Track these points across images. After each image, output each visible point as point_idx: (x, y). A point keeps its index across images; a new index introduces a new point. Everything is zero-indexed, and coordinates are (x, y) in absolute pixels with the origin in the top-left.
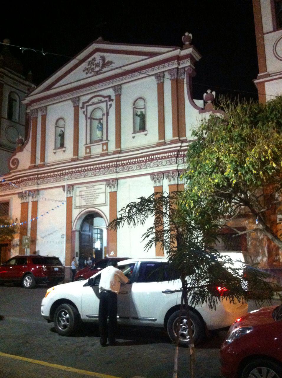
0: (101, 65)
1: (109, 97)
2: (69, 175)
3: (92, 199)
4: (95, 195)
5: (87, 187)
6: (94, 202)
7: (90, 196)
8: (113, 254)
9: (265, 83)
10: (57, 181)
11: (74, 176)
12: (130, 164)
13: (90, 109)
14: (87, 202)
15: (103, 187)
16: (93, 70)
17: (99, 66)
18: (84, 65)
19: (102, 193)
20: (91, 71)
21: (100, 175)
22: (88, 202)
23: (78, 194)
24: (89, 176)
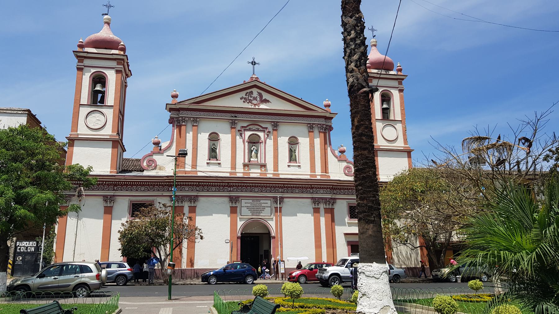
0: (258, 99)
1: (267, 128)
2: (234, 187)
3: (258, 211)
4: (261, 208)
5: (253, 200)
6: (260, 214)
7: (256, 209)
9: (378, 151)
13: (248, 134)
16: (250, 101)
17: (257, 100)
18: (243, 94)
19: (268, 207)
20: (248, 101)
21: (266, 192)
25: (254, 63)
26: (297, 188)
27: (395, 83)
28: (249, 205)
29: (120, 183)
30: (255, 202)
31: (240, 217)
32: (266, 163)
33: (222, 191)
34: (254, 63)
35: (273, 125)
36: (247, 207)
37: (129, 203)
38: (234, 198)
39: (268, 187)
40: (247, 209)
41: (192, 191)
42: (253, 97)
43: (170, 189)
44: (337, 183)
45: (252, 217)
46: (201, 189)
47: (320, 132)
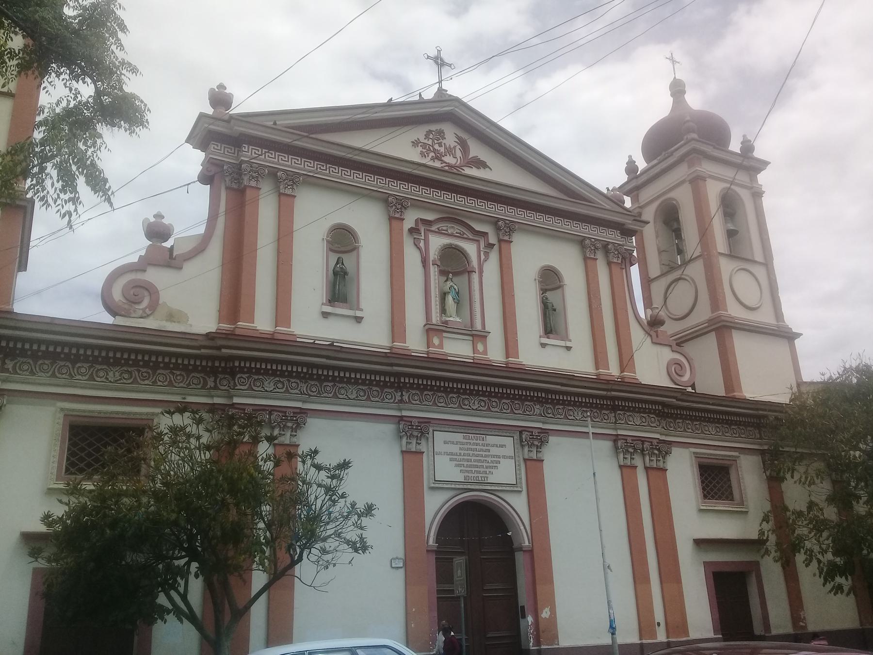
0: (459, 154)
1: (484, 234)
3: (482, 470)
4: (489, 459)
6: (487, 477)
8: (549, 613)
9: (733, 330)
10: (372, 399)
11: (428, 396)
12: (569, 405)
13: (436, 243)
14: (467, 474)
15: (508, 441)
16: (438, 155)
18: (419, 133)
22: (470, 475)
23: (439, 446)
24: (475, 408)
25: (439, 62)
26: (578, 406)
27: (742, 177)
28: (455, 449)
29: (31, 346)
30: (472, 442)
31: (433, 485)
32: (487, 329)
33: (377, 399)
34: (439, 62)
35: (498, 229)
36: (452, 454)
37: (61, 421)
38: (415, 422)
39: (507, 398)
40: (451, 460)
41: (287, 391)
42: (446, 148)
43: (211, 383)
44: (678, 400)
45: (465, 487)
46: (314, 389)
47: (609, 264)
